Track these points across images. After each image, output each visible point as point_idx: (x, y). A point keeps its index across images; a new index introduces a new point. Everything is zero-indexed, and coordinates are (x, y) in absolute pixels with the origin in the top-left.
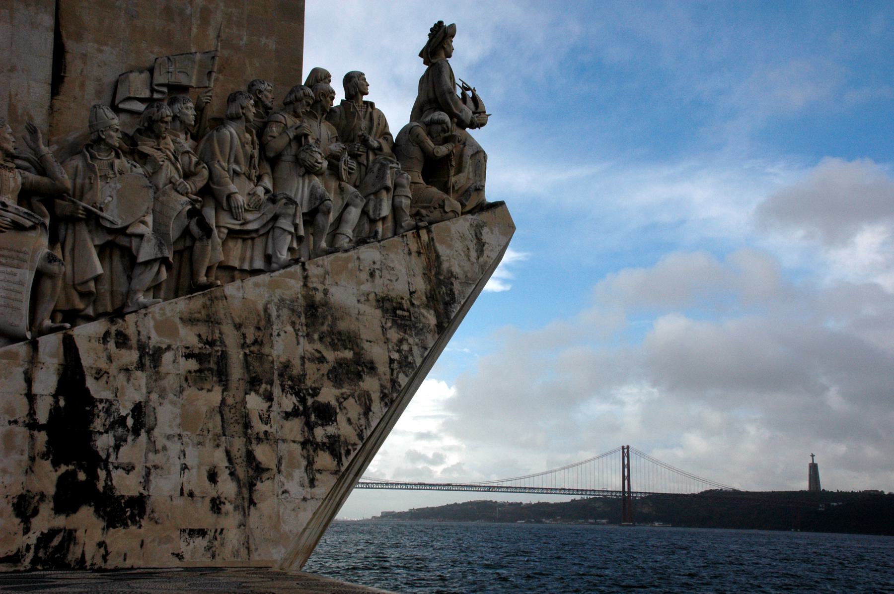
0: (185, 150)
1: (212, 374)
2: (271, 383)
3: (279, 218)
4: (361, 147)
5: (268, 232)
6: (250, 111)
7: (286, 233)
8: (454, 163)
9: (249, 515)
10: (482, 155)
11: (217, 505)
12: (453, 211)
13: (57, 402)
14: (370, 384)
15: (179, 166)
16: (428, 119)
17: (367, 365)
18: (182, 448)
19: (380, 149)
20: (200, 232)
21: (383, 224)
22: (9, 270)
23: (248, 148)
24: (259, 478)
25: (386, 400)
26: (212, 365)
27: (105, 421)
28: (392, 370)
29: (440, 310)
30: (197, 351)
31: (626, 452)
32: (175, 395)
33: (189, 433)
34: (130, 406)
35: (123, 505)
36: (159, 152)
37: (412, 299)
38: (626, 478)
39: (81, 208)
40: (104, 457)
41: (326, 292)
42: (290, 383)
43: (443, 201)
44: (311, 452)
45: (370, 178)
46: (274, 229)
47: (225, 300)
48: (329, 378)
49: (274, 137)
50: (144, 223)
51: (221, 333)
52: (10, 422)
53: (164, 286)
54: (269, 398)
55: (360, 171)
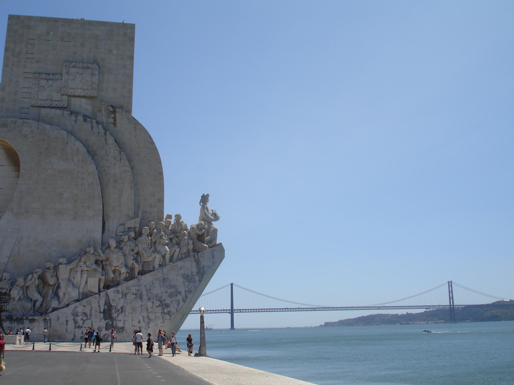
2: (153, 299)
5: (154, 260)
14: (180, 297)
19: (185, 234)
25: (184, 301)
26: (139, 296)
30: (135, 293)
31: (450, 284)
34: (120, 307)
38: (451, 298)
40: (115, 318)
41: (168, 275)
44: (164, 315)
45: (182, 242)
48: (168, 296)
51: (141, 288)
54: (153, 303)
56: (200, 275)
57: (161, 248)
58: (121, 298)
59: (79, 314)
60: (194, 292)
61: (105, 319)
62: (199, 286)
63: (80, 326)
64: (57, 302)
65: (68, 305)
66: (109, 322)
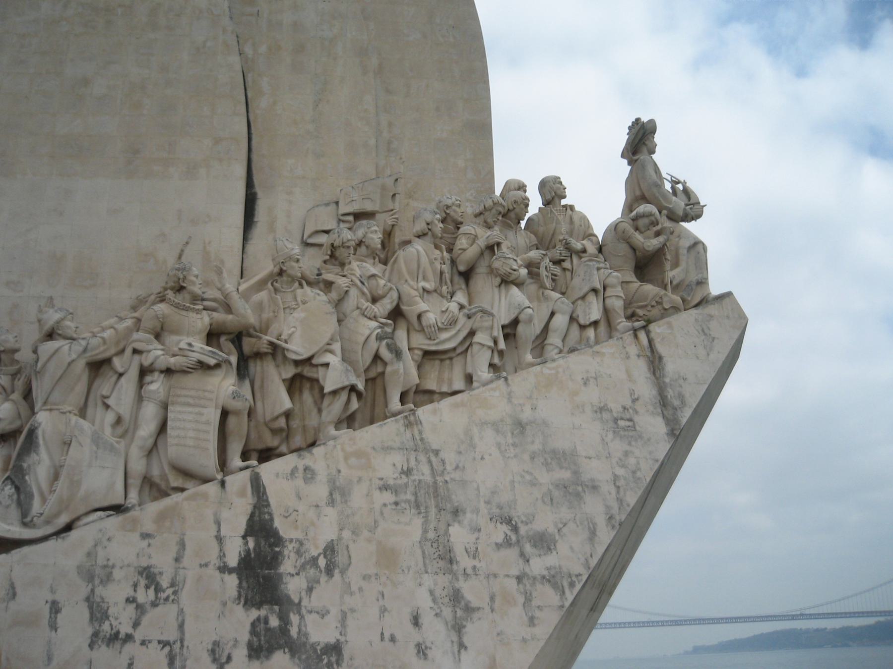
0: (371, 273)
1: (410, 506)
3: (477, 333)
4: (563, 252)
6: (437, 226)
7: (485, 348)
8: (668, 257)
9: (460, 659)
10: (700, 247)
11: (422, 650)
12: (672, 307)
13: (246, 543)
14: (594, 507)
15: (365, 290)
16: (634, 213)
17: (587, 483)
18: (381, 588)
19: (584, 251)
20: (390, 355)
21: (596, 330)
22: (197, 410)
23: (438, 266)
24: (469, 619)
25: (613, 522)
26: (410, 497)
27: (296, 562)
28: (618, 487)
29: (667, 416)
30: (391, 482)
32: (370, 531)
33: (386, 572)
35: (319, 652)
36: (344, 278)
37: (635, 407)
39: (265, 342)
40: (296, 601)
41: (534, 409)
42: (498, 510)
43: (661, 298)
44: (528, 587)
45: (577, 281)
46: (472, 346)
47: (420, 426)
48: (544, 502)
49: (464, 250)
50: (332, 352)
52: (201, 566)
53: (359, 417)
55: (566, 276)
56: (669, 413)
57: (497, 297)
58: (328, 504)
59: (117, 574)
60: (649, 488)
61: (249, 603)
62: (666, 461)
63: (118, 632)
64: (14, 513)
65: (68, 528)
66: (266, 621)
